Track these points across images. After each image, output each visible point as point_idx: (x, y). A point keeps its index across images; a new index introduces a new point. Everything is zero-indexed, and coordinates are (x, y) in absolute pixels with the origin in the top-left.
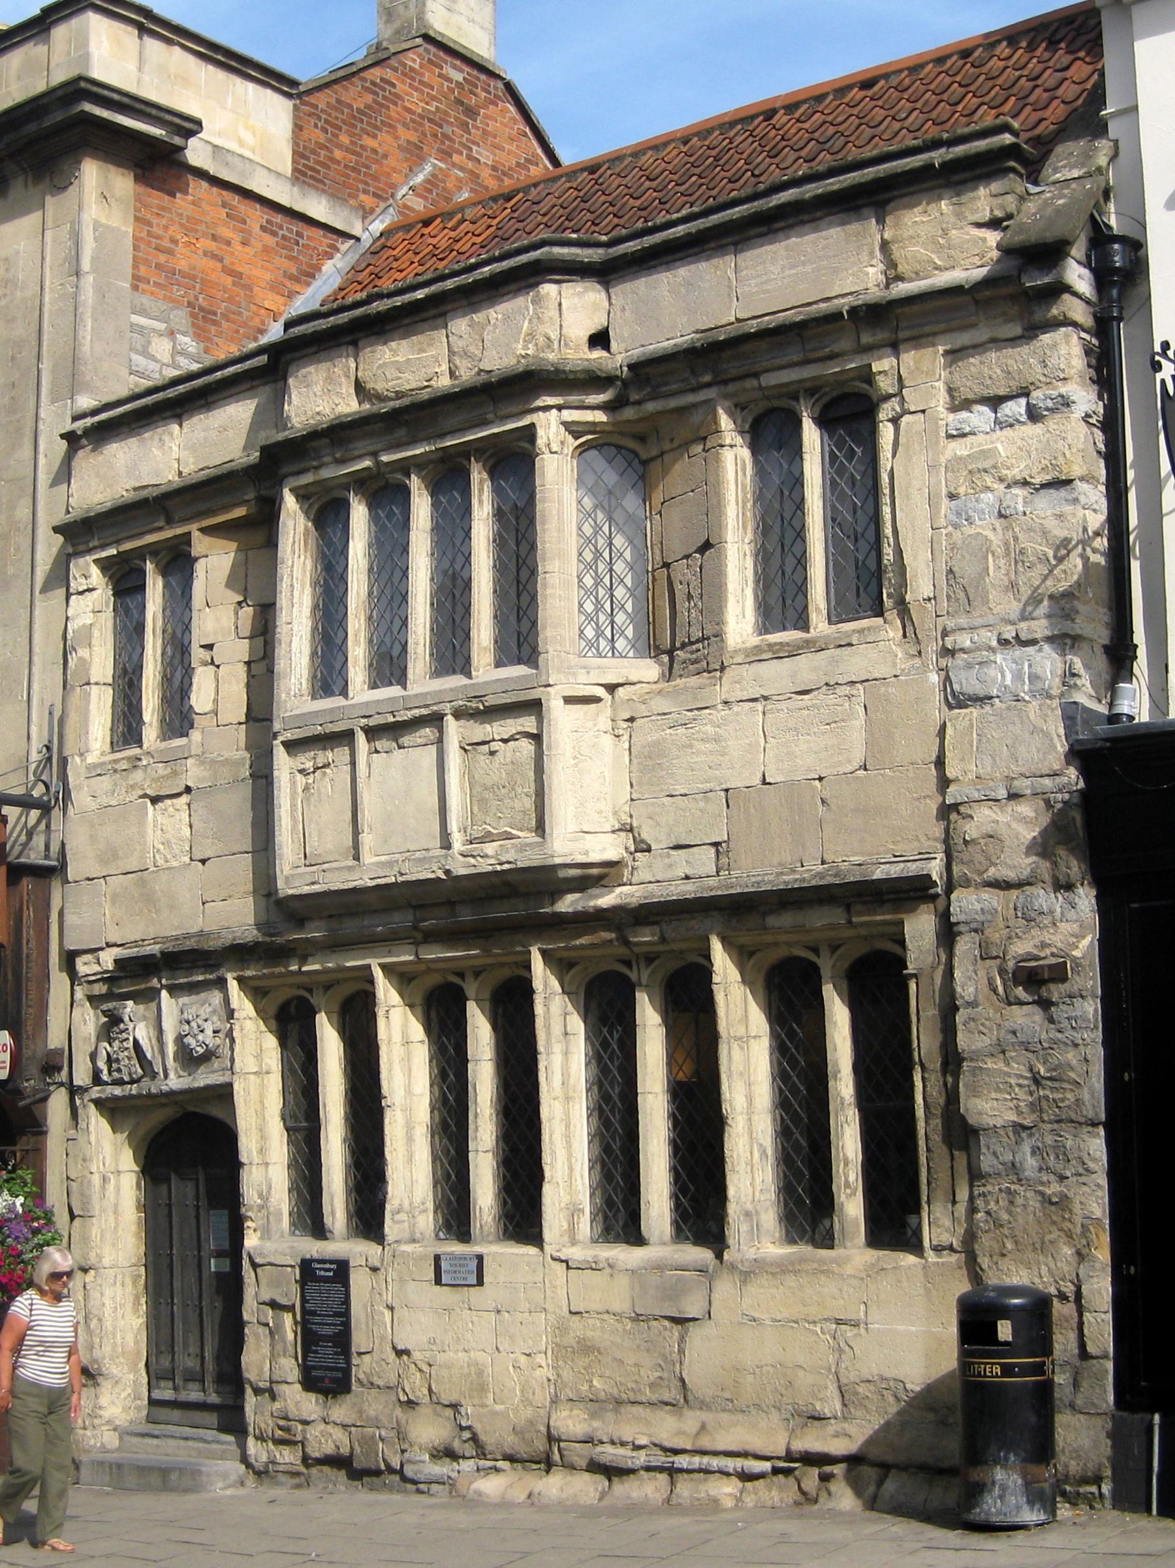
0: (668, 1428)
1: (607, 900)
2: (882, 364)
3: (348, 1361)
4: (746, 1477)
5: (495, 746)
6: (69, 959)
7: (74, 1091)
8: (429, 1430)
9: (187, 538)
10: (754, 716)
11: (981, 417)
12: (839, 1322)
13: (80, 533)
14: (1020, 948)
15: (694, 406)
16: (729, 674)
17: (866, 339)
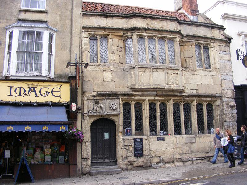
0: (190, 156)
1: (184, 94)
2: (212, 44)
3: (142, 152)
4: (201, 160)
5: (171, 74)
6: (83, 92)
7: (83, 114)
8: (156, 160)
9: (108, 35)
10: (200, 77)
11: (221, 52)
12: (211, 142)
13: (86, 28)
14: (230, 104)
15: (191, 42)
16: (197, 72)
17: (211, 41)
